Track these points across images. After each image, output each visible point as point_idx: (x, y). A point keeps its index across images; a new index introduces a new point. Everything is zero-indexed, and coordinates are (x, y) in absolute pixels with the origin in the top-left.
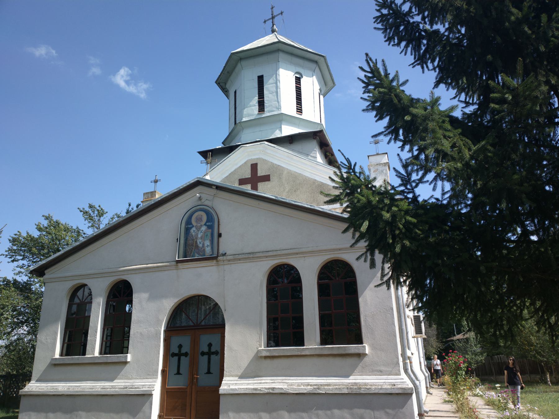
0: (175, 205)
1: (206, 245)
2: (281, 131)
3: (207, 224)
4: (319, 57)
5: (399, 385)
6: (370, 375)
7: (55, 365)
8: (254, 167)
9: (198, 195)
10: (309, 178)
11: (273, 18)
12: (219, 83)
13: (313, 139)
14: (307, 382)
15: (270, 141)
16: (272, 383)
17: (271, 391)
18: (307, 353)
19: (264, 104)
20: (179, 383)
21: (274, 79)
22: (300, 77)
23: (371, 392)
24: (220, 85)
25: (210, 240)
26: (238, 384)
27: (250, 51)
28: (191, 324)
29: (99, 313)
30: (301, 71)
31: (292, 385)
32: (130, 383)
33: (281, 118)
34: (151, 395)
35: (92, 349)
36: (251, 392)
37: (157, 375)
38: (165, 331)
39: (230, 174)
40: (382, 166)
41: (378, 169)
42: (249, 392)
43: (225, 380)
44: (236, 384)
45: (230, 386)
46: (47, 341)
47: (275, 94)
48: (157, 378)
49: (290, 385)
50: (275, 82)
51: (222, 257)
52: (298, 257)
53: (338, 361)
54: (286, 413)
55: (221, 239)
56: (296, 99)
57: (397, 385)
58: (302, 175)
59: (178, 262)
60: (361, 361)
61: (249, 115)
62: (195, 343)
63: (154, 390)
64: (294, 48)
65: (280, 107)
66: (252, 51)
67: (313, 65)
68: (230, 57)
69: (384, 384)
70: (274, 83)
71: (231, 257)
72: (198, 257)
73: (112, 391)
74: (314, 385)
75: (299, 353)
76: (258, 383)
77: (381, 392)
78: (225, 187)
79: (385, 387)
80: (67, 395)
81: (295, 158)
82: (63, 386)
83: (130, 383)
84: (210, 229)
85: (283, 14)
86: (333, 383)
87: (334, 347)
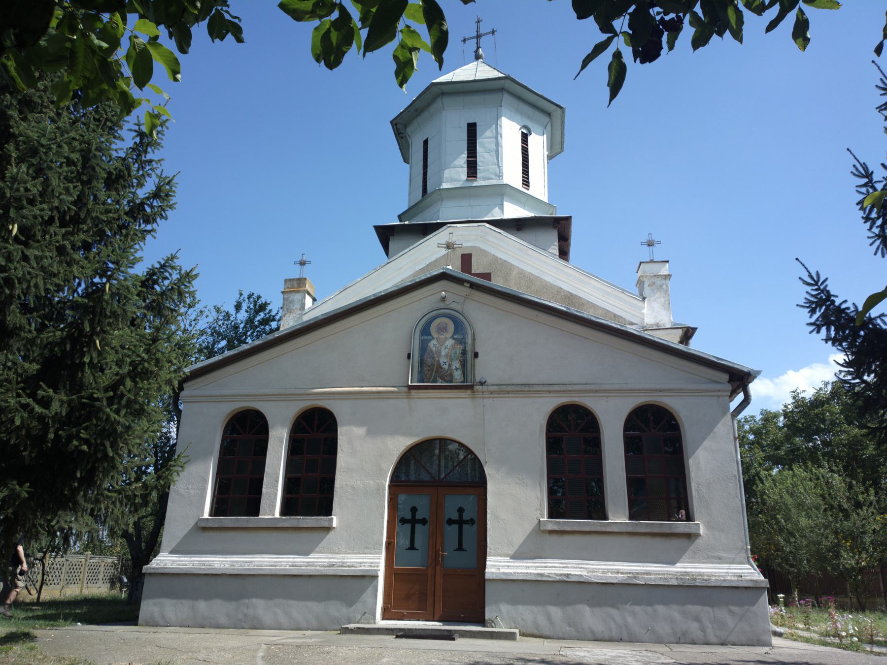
2: (502, 209)
3: (456, 336)
4: (555, 107)
6: (704, 563)
7: (205, 529)
9: (443, 293)
10: (551, 285)
11: (478, 37)
13: (553, 227)
14: (616, 569)
15: (488, 222)
16: (563, 567)
18: (615, 529)
19: (476, 167)
22: (528, 133)
23: (710, 585)
24: (397, 128)
25: (460, 361)
26: (511, 566)
27: (460, 85)
28: (425, 477)
29: (282, 454)
30: (530, 125)
31: (594, 572)
32: (337, 558)
33: (502, 192)
34: (376, 577)
35: (271, 507)
36: (534, 579)
37: (381, 549)
38: (390, 486)
40: (660, 278)
42: (531, 579)
43: (490, 561)
44: (508, 566)
47: (494, 153)
48: (381, 554)
50: (494, 135)
51: (481, 387)
53: (659, 542)
54: (587, 608)
55: (477, 361)
56: (523, 166)
58: (541, 279)
59: (411, 388)
60: (692, 544)
61: (452, 180)
62: (437, 506)
67: (545, 119)
70: (493, 137)
71: (492, 388)
73: (311, 570)
74: (627, 573)
75: (603, 529)
76: (542, 567)
77: (724, 584)
79: (729, 578)
80: (230, 575)
81: (531, 252)
82: (222, 561)
83: (337, 558)
85: (495, 33)
86: (652, 570)
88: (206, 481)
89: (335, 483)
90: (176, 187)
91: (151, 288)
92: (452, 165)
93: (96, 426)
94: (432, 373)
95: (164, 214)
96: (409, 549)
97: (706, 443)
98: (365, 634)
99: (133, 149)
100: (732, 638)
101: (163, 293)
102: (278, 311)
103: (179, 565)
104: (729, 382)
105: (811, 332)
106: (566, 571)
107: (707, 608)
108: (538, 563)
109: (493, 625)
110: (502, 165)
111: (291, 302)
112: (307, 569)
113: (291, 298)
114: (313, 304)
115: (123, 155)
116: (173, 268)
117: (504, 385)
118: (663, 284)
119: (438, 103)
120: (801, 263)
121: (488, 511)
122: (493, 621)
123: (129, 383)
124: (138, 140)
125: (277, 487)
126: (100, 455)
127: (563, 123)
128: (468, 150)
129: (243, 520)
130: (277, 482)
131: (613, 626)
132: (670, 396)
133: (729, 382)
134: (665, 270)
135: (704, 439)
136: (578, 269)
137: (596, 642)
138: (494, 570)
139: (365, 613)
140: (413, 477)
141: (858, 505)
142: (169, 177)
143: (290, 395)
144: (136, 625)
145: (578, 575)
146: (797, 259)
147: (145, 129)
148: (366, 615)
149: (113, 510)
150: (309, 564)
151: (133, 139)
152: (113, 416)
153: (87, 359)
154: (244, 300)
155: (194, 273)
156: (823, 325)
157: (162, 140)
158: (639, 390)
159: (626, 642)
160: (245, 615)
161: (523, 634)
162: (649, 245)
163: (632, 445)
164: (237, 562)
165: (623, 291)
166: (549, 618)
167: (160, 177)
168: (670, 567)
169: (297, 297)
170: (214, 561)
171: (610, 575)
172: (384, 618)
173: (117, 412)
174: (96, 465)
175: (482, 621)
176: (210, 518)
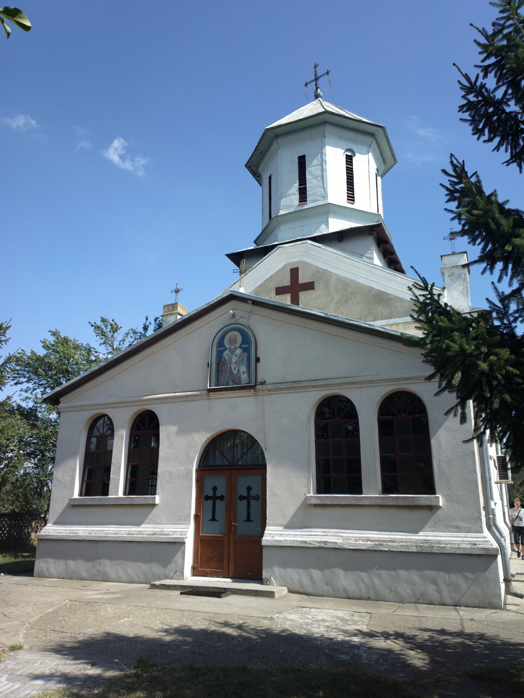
0: (205, 323)
1: (242, 372)
2: (327, 225)
3: (243, 346)
4: (375, 128)
5: (481, 544)
6: (444, 532)
7: (74, 506)
8: (294, 272)
9: (231, 311)
11: (316, 79)
12: (250, 167)
14: (366, 537)
15: (314, 239)
16: (324, 535)
17: (323, 545)
18: (366, 502)
23: (445, 552)
24: (251, 169)
27: (289, 126)
29: (122, 448)
31: (348, 539)
34: (183, 543)
37: (190, 521)
38: (197, 471)
39: (265, 281)
41: (454, 273)
42: (297, 545)
43: (268, 530)
44: (281, 535)
45: (273, 537)
46: (64, 479)
47: (320, 178)
49: (345, 539)
51: (261, 386)
52: (354, 387)
53: (405, 514)
55: (259, 365)
56: (347, 184)
57: (478, 544)
58: (355, 281)
59: (209, 391)
60: (433, 515)
61: (287, 207)
62: (232, 486)
63: (186, 538)
64: (344, 119)
65: (326, 195)
66: (292, 125)
67: (369, 139)
68: (264, 134)
69: (463, 542)
71: (272, 386)
73: (139, 537)
74: (375, 541)
75: (356, 503)
76: (307, 535)
77: (458, 552)
79: (463, 546)
80: (89, 541)
81: (345, 260)
84: (246, 352)
85: (329, 73)
86: (397, 538)
87: (399, 497)
89: (158, 469)
94: (225, 378)
98: (166, 589)
100: (465, 600)
103: (57, 533)
107: (442, 574)
109: (268, 583)
110: (327, 187)
117: (279, 383)
118: (462, 273)
119: (275, 144)
122: (268, 580)
128: (299, 179)
131: (362, 586)
132: (415, 383)
139: (177, 571)
143: (127, 402)
144: (33, 576)
148: (178, 573)
150: (140, 533)
158: (388, 380)
160: (98, 571)
164: (93, 531)
166: (311, 577)
168: (415, 536)
170: (79, 530)
175: (259, 579)
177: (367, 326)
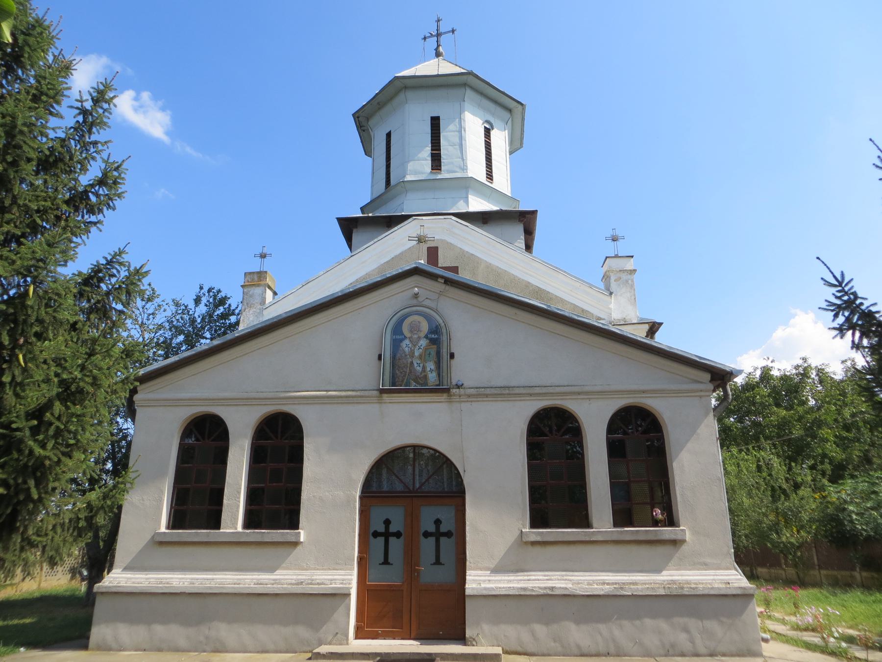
1: (428, 369)
2: (467, 202)
4: (516, 104)
6: (690, 570)
7: (161, 543)
12: (358, 117)
14: (601, 580)
16: (547, 580)
17: (550, 593)
18: (600, 538)
20: (392, 576)
21: (456, 125)
23: (698, 593)
24: (358, 120)
25: (435, 362)
28: (399, 487)
30: (492, 121)
31: (579, 583)
32: (306, 575)
33: (466, 184)
34: (349, 595)
37: (353, 565)
38: (361, 498)
42: (514, 593)
43: (470, 575)
44: (489, 581)
45: (480, 584)
47: (457, 147)
48: (353, 569)
50: (458, 129)
51: (457, 390)
53: (644, 552)
55: (453, 362)
56: (486, 160)
57: (732, 583)
58: (509, 273)
59: (382, 391)
61: (416, 173)
62: (412, 518)
66: (427, 79)
67: (506, 115)
68: (391, 82)
70: (456, 131)
72: (415, 386)
73: (277, 588)
74: (613, 584)
78: (457, 281)
79: (716, 586)
82: (180, 579)
83: (306, 575)
84: (434, 344)
86: (640, 580)
87: (639, 530)
88: (162, 492)
90: (125, 174)
91: (96, 286)
92: (416, 158)
93: (17, 460)
94: (405, 376)
95: (111, 204)
96: (383, 564)
97: (689, 445)
99: (75, 129)
100: (721, 648)
101: (108, 293)
102: (238, 305)
103: (134, 583)
104: (710, 381)
105: (834, 338)
106: (550, 584)
108: (520, 576)
109: (474, 643)
111: (251, 296)
112: (273, 588)
113: (251, 293)
114: (274, 298)
115: (63, 135)
116: (121, 264)
117: (482, 388)
118: (629, 279)
119: (402, 96)
120: (823, 262)
121: (467, 523)
122: (474, 639)
123: (58, 407)
124: (80, 119)
125: (239, 498)
126: (22, 497)
127: (523, 119)
128: (432, 143)
129: (203, 534)
130: (239, 493)
133: (710, 381)
134: (630, 265)
135: (687, 441)
136: (546, 263)
137: (583, 658)
138: (474, 586)
139: (337, 633)
140: (385, 488)
141: (797, 486)
142: (118, 162)
143: (251, 399)
145: (563, 588)
146: (818, 258)
147: (88, 105)
148: (338, 635)
149: (53, 537)
150: (276, 581)
151: (74, 117)
152: (38, 451)
153: (6, 379)
154: (204, 295)
155: (144, 270)
156: (848, 330)
157: (109, 118)
159: (614, 656)
160: (207, 638)
161: (506, 652)
162: (613, 240)
163: (615, 450)
165: (591, 286)
166: (533, 633)
167: (106, 162)
169: (257, 291)
170: (172, 578)
171: (596, 586)
172: (357, 637)
173: (43, 446)
174: (19, 508)
176: (167, 531)
177: (601, 325)
